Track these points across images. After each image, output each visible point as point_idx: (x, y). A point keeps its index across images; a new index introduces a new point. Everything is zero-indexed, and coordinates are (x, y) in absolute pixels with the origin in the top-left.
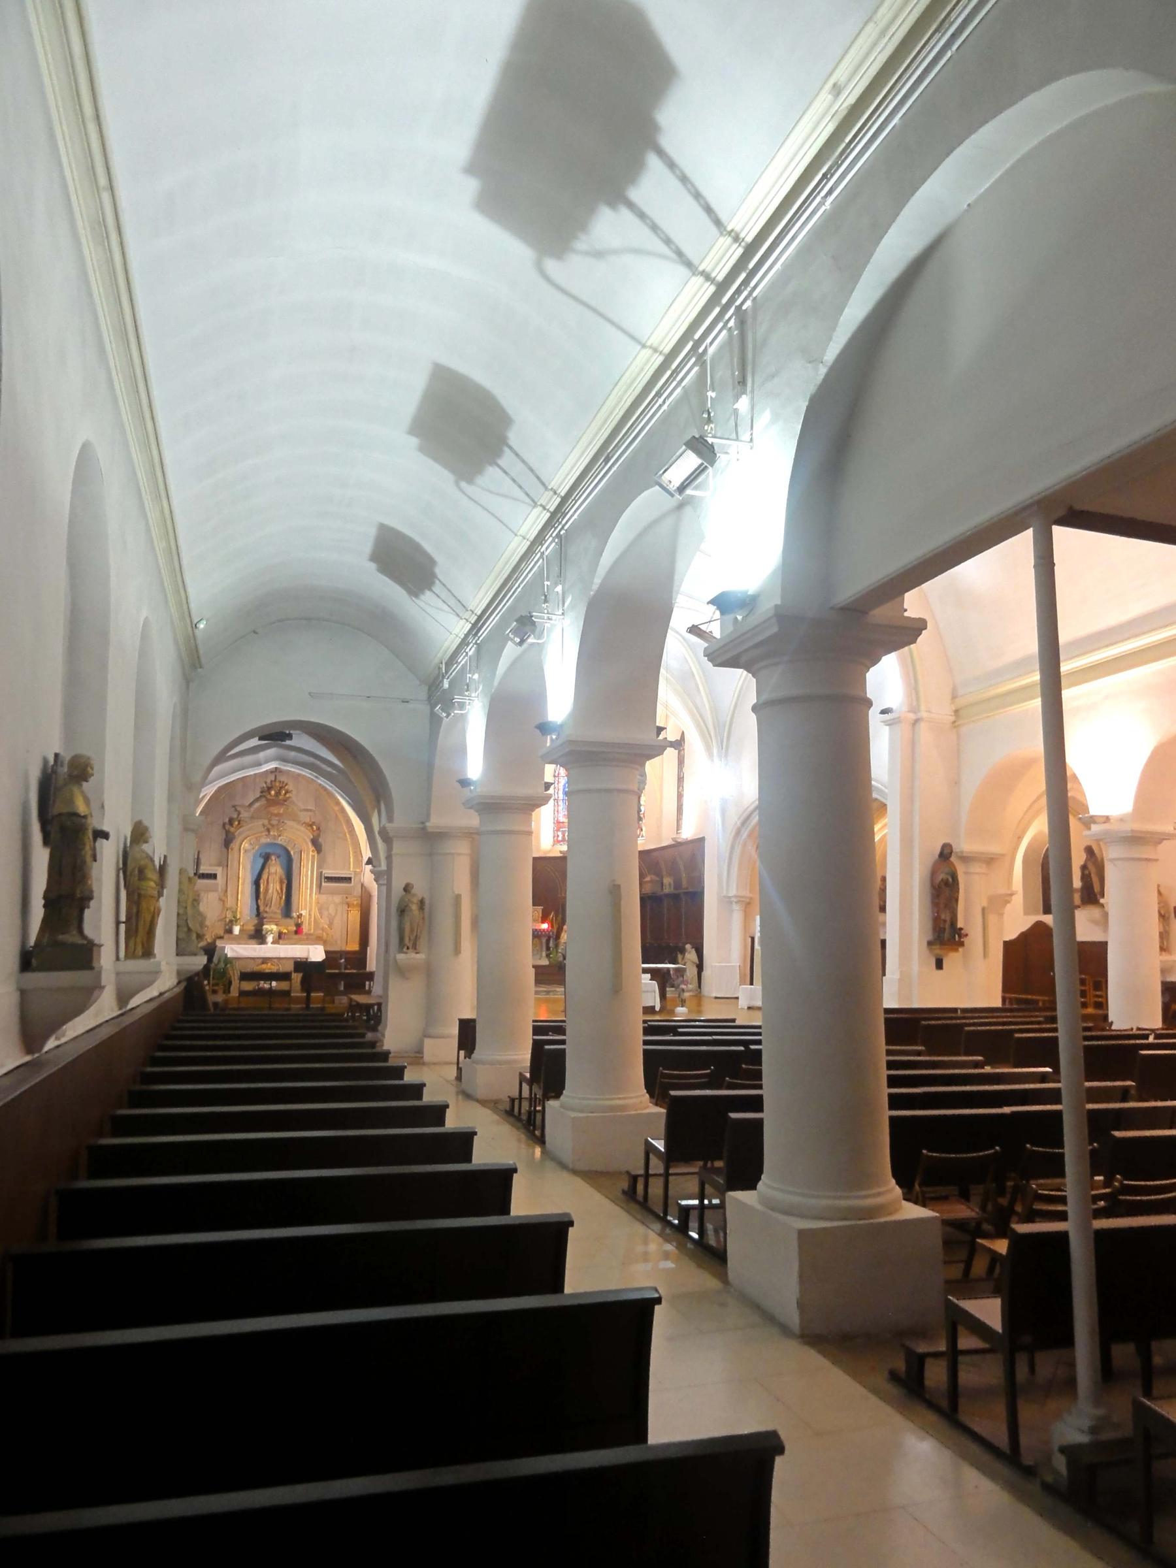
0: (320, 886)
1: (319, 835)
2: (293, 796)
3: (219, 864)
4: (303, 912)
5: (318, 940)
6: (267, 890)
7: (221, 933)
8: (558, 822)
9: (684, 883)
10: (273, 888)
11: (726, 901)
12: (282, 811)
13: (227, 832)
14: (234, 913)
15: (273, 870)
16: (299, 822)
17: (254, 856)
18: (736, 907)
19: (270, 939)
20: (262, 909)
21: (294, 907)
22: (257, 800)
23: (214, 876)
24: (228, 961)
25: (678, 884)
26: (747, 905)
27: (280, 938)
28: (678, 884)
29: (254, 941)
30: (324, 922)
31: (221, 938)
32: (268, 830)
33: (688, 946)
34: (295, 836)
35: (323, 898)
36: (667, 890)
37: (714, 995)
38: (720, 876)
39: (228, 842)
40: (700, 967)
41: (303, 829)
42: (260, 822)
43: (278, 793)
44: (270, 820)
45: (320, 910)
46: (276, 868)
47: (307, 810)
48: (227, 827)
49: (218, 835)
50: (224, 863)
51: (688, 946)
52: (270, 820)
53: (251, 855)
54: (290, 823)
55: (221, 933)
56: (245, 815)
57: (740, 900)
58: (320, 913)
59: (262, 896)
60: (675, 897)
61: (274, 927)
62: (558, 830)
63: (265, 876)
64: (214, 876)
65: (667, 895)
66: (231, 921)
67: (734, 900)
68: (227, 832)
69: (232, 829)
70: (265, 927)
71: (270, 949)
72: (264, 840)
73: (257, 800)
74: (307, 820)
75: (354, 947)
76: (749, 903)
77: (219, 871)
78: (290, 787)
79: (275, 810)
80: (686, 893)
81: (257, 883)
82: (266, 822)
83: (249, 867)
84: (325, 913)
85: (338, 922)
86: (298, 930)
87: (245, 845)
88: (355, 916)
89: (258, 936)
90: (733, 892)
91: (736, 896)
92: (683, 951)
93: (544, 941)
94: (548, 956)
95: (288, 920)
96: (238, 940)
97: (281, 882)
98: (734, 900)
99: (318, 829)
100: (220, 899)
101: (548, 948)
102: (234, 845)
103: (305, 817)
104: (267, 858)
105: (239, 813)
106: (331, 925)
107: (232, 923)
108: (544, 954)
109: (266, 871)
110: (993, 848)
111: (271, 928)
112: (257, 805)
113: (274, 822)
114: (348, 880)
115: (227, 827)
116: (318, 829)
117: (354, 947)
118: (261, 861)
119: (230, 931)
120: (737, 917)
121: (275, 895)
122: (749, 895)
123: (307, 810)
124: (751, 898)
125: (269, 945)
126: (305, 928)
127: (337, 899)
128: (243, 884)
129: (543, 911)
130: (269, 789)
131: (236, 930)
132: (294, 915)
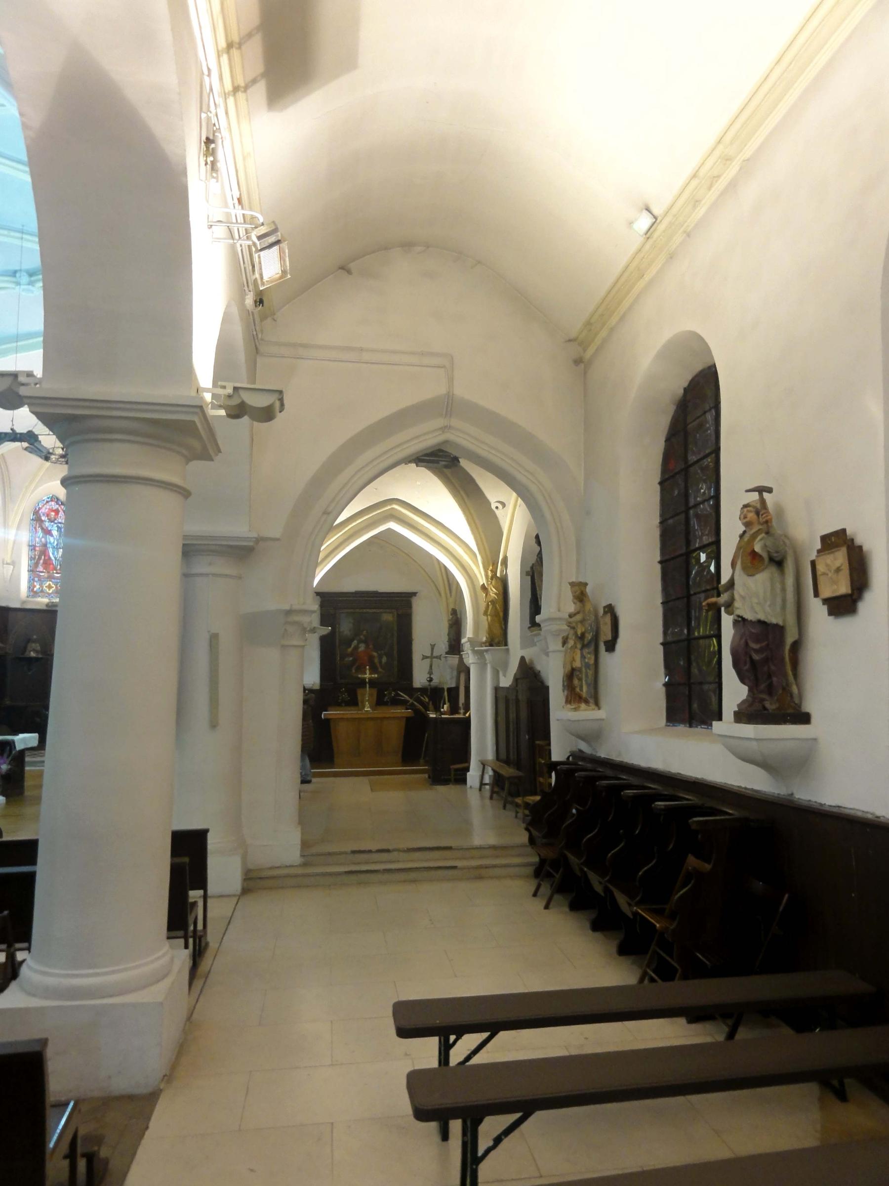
110: (237, 528)
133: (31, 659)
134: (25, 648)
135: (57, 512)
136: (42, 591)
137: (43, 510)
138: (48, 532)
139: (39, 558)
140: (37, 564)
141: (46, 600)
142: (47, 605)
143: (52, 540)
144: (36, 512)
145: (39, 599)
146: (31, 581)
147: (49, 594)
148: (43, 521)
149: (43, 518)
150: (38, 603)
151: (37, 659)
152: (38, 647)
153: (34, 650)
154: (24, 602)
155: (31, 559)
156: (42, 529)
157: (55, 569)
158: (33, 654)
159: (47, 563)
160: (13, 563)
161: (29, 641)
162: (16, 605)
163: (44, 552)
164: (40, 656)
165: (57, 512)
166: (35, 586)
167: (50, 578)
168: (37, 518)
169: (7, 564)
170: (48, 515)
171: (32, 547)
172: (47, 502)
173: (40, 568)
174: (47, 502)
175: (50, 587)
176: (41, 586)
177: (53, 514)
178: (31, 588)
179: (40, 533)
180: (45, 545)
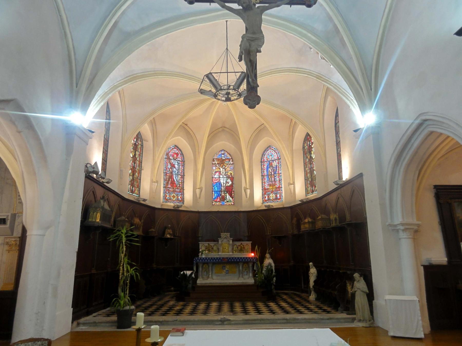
8: (265, 189)
9: (348, 218)
11: (392, 229)
18: (402, 235)
25: (342, 218)
26: (416, 232)
28: (342, 218)
33: (356, 275)
36: (334, 225)
37: (391, 334)
38: (382, 205)
40: (370, 296)
51: (356, 275)
57: (407, 228)
60: (341, 230)
62: (265, 194)
65: (334, 228)
67: (402, 228)
76: (416, 231)
80: (349, 225)
90: (398, 219)
91: (402, 224)
92: (352, 280)
93: (251, 265)
94: (254, 276)
98: (402, 228)
101: (254, 271)
108: (251, 275)
117: (10, 288)
120: (406, 245)
122: (415, 221)
124: (418, 225)
129: (252, 244)
133: (168, 238)
134: (164, 233)
135: (177, 154)
136: (170, 199)
137: (171, 153)
138: (173, 166)
139: (169, 180)
140: (168, 183)
141: (172, 204)
142: (174, 207)
143: (175, 169)
144: (167, 154)
145: (169, 204)
146: (165, 192)
147: (174, 201)
148: (170, 159)
149: (171, 158)
150: (168, 205)
151: (171, 239)
152: (170, 231)
153: (170, 234)
154: (162, 205)
155: (165, 180)
156: (170, 163)
157: (176, 186)
158: (168, 236)
159: (173, 183)
160: (157, 182)
161: (166, 228)
162: (159, 207)
163: (171, 177)
164: (172, 237)
165: (177, 154)
166: (166, 196)
167: (174, 191)
168: (168, 158)
169: (154, 182)
170: (173, 156)
171: (166, 174)
172: (173, 149)
173: (169, 186)
174: (173, 149)
175: (174, 197)
176: (170, 196)
177: (175, 155)
178: (165, 197)
179: (169, 166)
180: (172, 173)
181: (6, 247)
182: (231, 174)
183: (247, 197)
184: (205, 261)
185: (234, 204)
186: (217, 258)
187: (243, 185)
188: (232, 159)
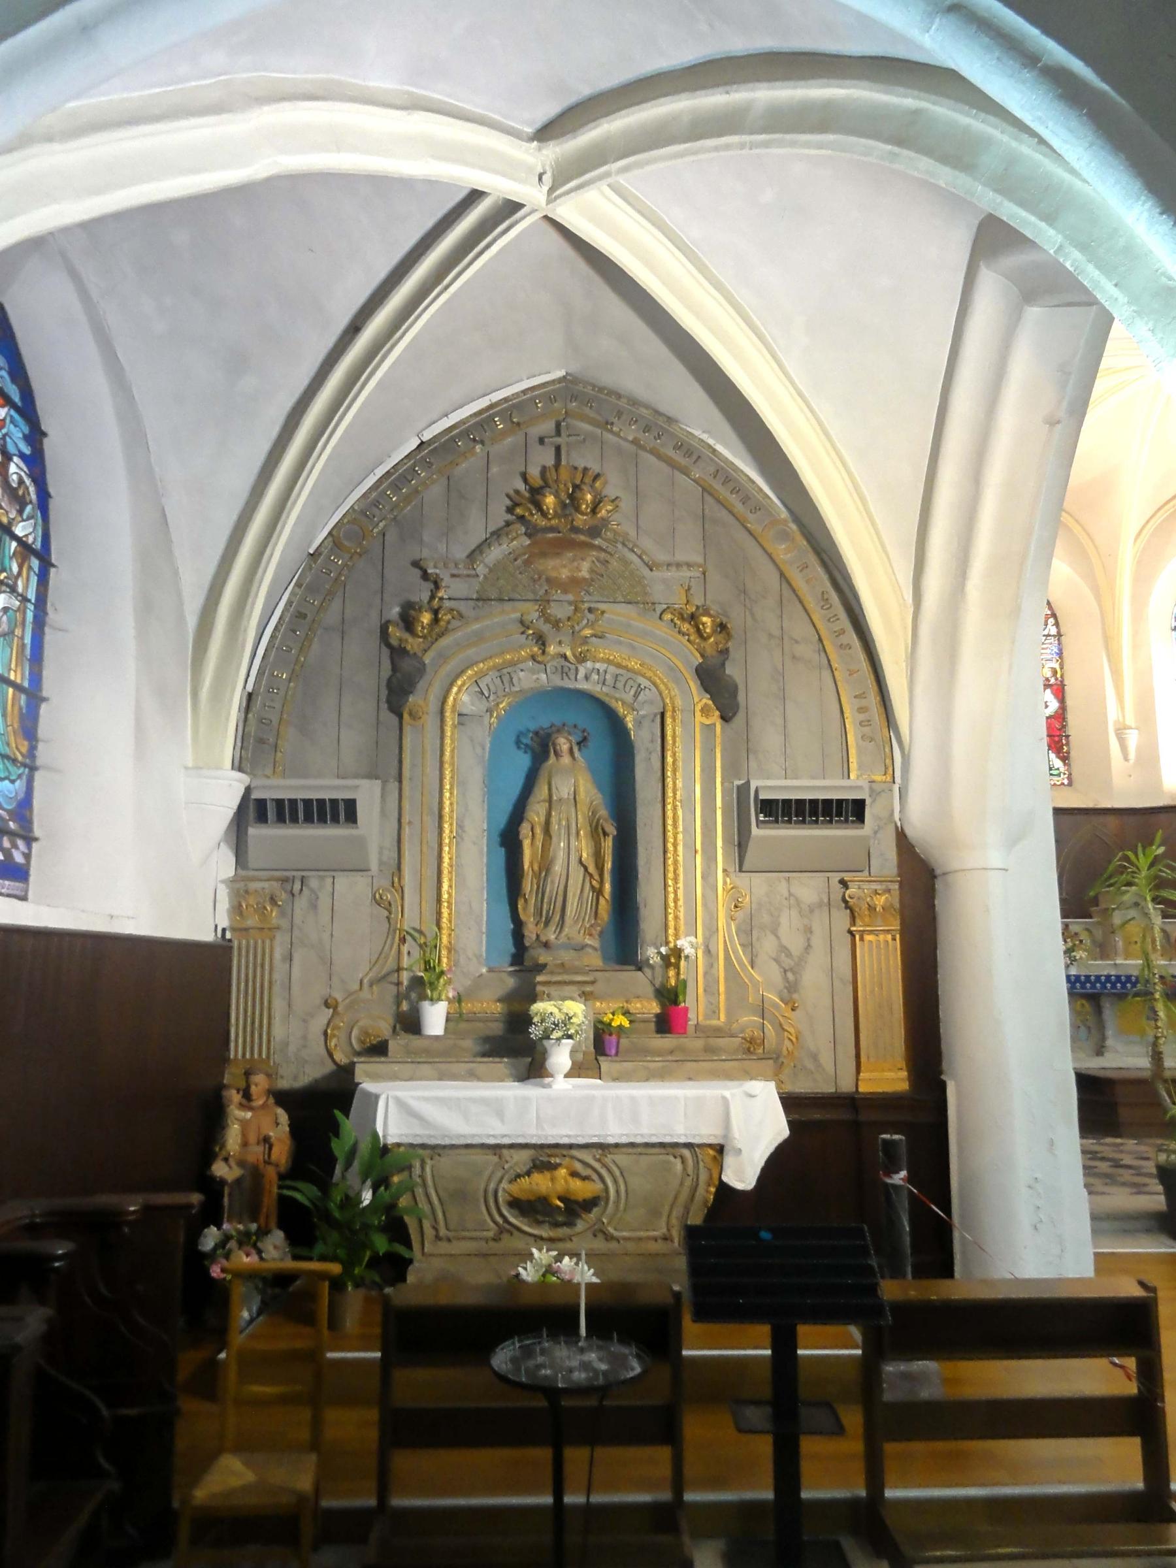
0: (741, 843)
1: (725, 652)
2: (620, 521)
3: (371, 775)
4: (685, 943)
5: (751, 1054)
6: (545, 866)
7: (383, 1027)
10: (569, 855)
12: (584, 573)
13: (398, 653)
14: (428, 947)
15: (563, 789)
16: (647, 605)
17: (496, 736)
19: (561, 1057)
20: (531, 931)
21: (649, 924)
22: (497, 534)
23: (345, 812)
24: (384, 1161)
27: (601, 1050)
29: (502, 1065)
30: (765, 980)
31: (379, 1049)
32: (541, 640)
34: (639, 660)
35: (756, 886)
39: (398, 691)
41: (663, 630)
42: (511, 613)
43: (572, 502)
44: (544, 602)
45: (748, 932)
46: (574, 784)
47: (678, 565)
48: (396, 633)
49: (364, 667)
50: (390, 767)
52: (544, 602)
53: (482, 734)
54: (617, 613)
55: (383, 1027)
56: (452, 588)
58: (748, 946)
59: (528, 885)
61: (576, 1009)
63: (536, 813)
64: (345, 812)
66: (417, 983)
68: (398, 653)
69: (413, 644)
70: (539, 1007)
71: (566, 1105)
72: (530, 678)
73: (497, 534)
74: (679, 600)
75: (888, 1076)
77: (369, 797)
78: (613, 486)
79: (561, 567)
81: (509, 840)
82: (532, 612)
83: (476, 776)
84: (767, 946)
85: (814, 980)
86: (669, 1019)
87: (462, 697)
88: (882, 955)
89: (515, 1046)
95: (630, 976)
96: (440, 1060)
97: (597, 832)
99: (722, 627)
100: (378, 901)
102: (422, 699)
103: (667, 587)
104: (541, 749)
105: (437, 585)
106: (791, 992)
107: (421, 988)
109: (541, 791)
111: (563, 1011)
112: (495, 553)
113: (559, 611)
114: (855, 810)
115: (396, 633)
116: (722, 627)
118: (523, 761)
119: (411, 1024)
121: (577, 875)
123: (678, 565)
125: (560, 1078)
126: (695, 1005)
127: (809, 889)
128: (458, 838)
130: (535, 495)
131: (435, 1017)
132: (651, 954)
181: (841, 919)
182: (1055, 672)
183: (1126, 759)
184: (1093, 986)
185: (1070, 784)
186: (1108, 977)
187: (1112, 714)
188: (1054, 615)
